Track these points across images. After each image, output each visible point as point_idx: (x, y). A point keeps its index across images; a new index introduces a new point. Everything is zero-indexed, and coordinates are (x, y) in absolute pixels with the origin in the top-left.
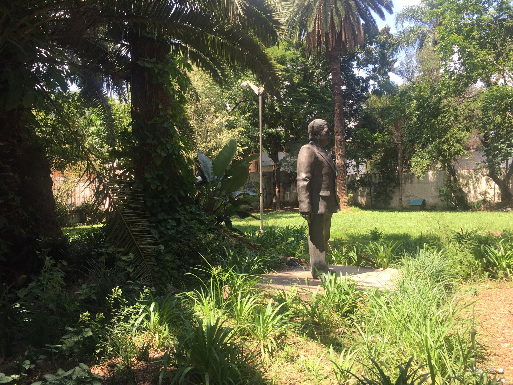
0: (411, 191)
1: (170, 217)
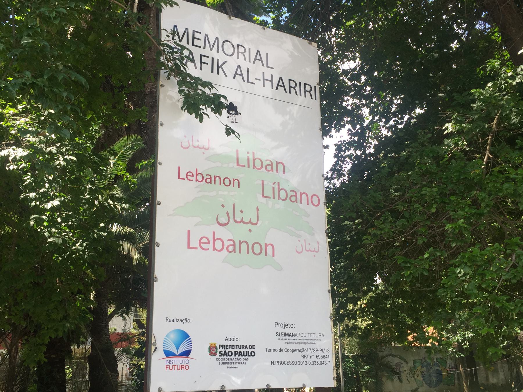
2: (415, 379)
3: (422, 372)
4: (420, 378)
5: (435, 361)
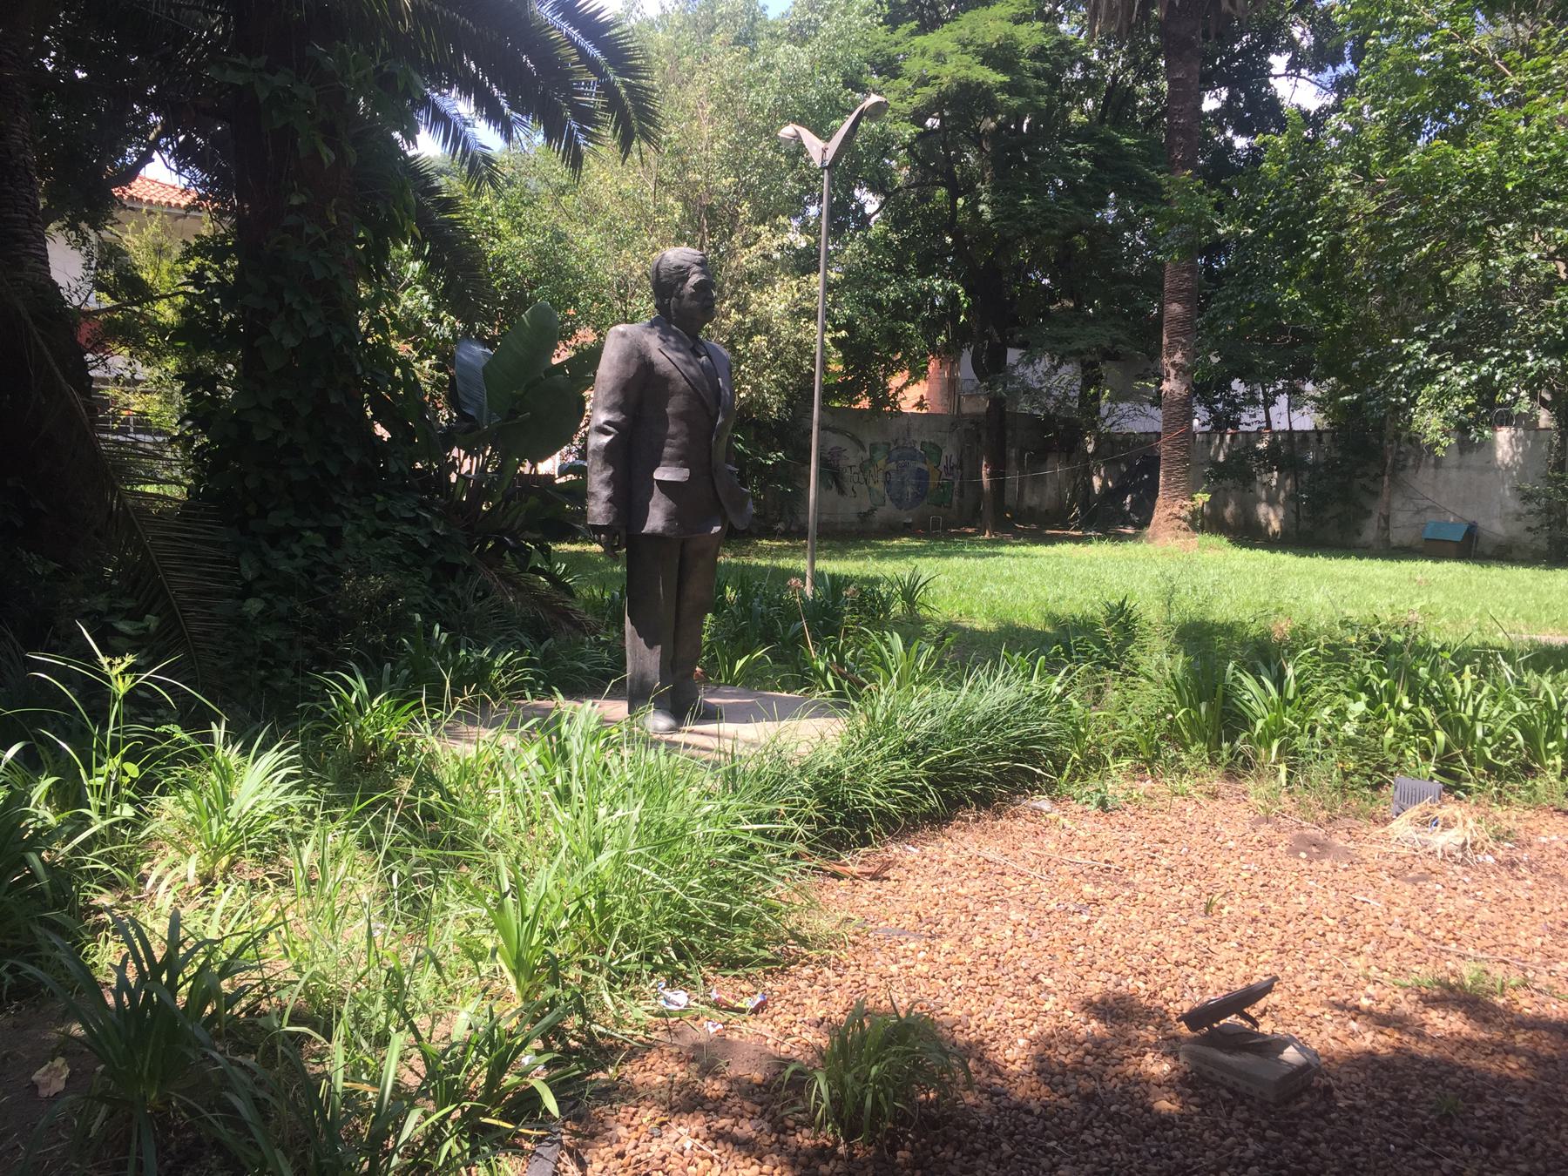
0: (1441, 496)
1: (309, 523)
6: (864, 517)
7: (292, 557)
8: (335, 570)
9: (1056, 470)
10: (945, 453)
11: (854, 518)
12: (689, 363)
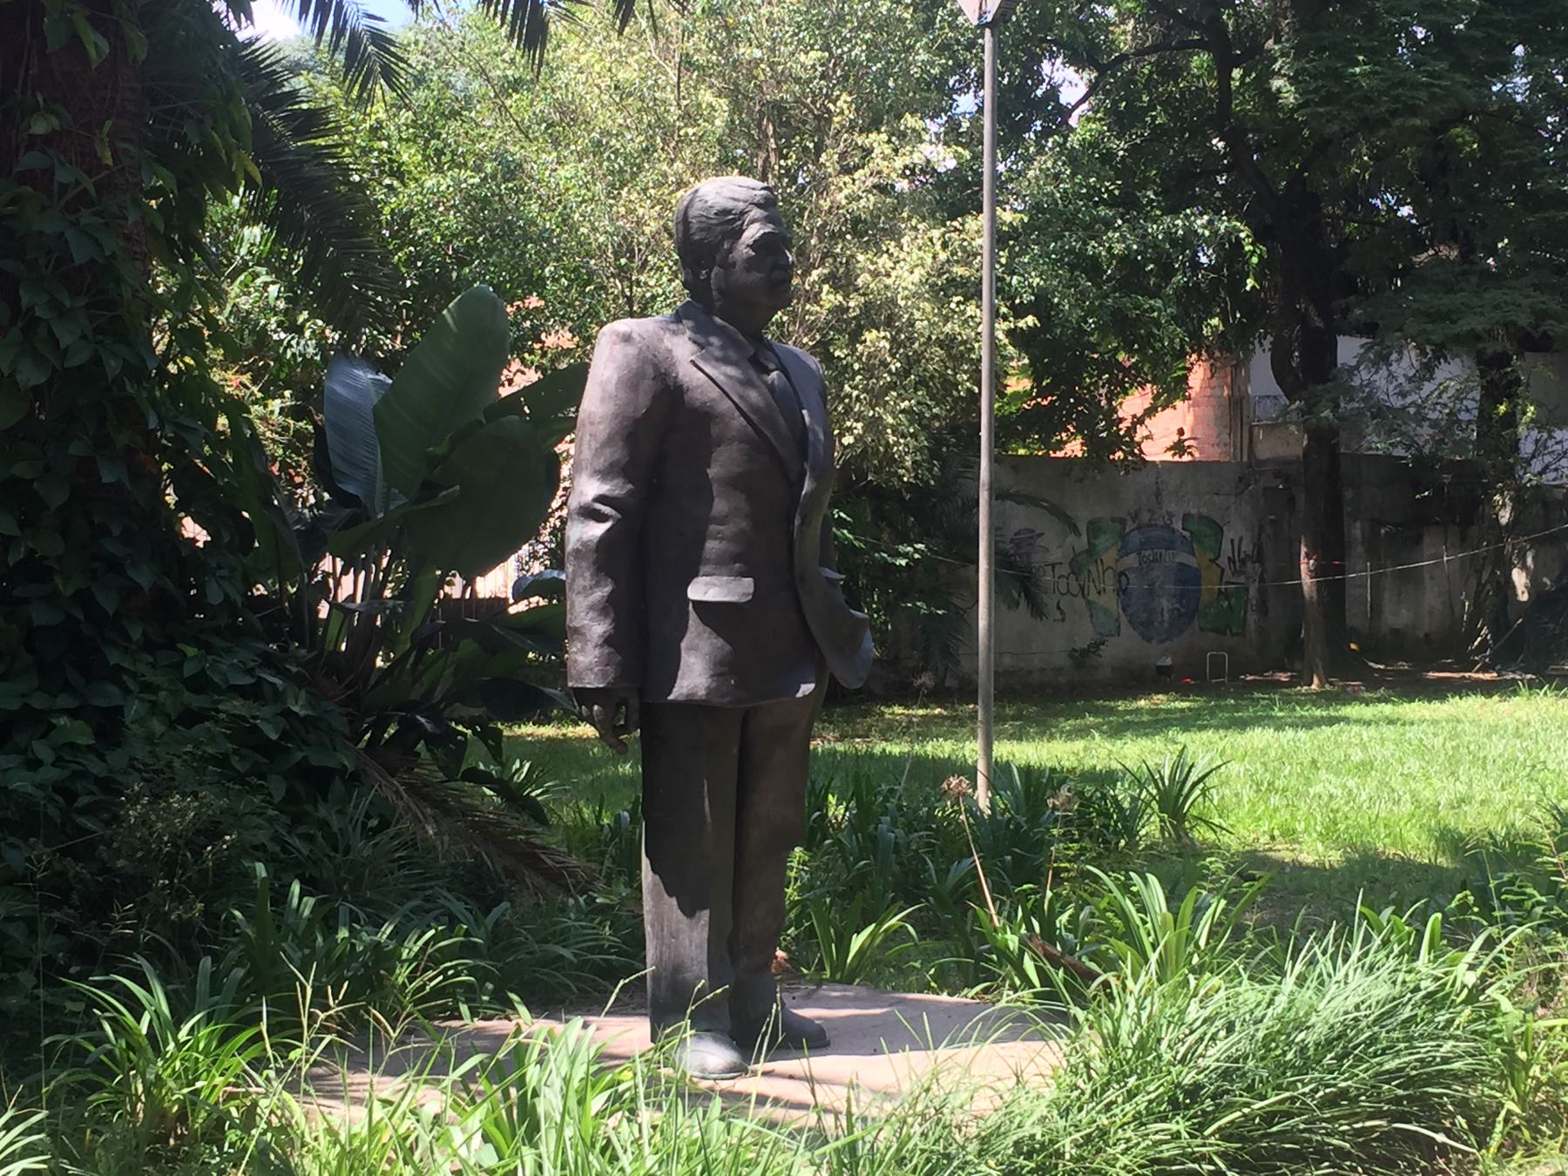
1: (64, 701)
2: (1089, 603)
3: (1122, 573)
4: (1109, 601)
5: (1178, 526)
6: (1082, 657)
7: (34, 764)
8: (109, 785)
9: (1440, 559)
10: (1229, 534)
11: (1062, 660)
12: (747, 383)
